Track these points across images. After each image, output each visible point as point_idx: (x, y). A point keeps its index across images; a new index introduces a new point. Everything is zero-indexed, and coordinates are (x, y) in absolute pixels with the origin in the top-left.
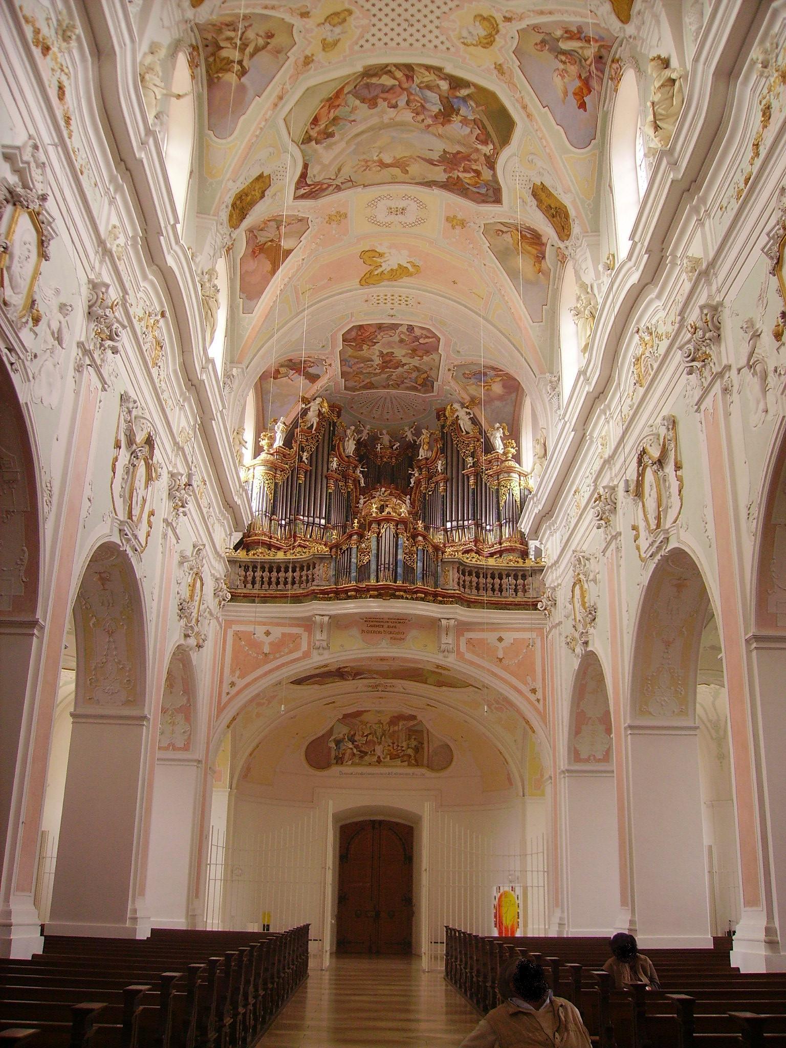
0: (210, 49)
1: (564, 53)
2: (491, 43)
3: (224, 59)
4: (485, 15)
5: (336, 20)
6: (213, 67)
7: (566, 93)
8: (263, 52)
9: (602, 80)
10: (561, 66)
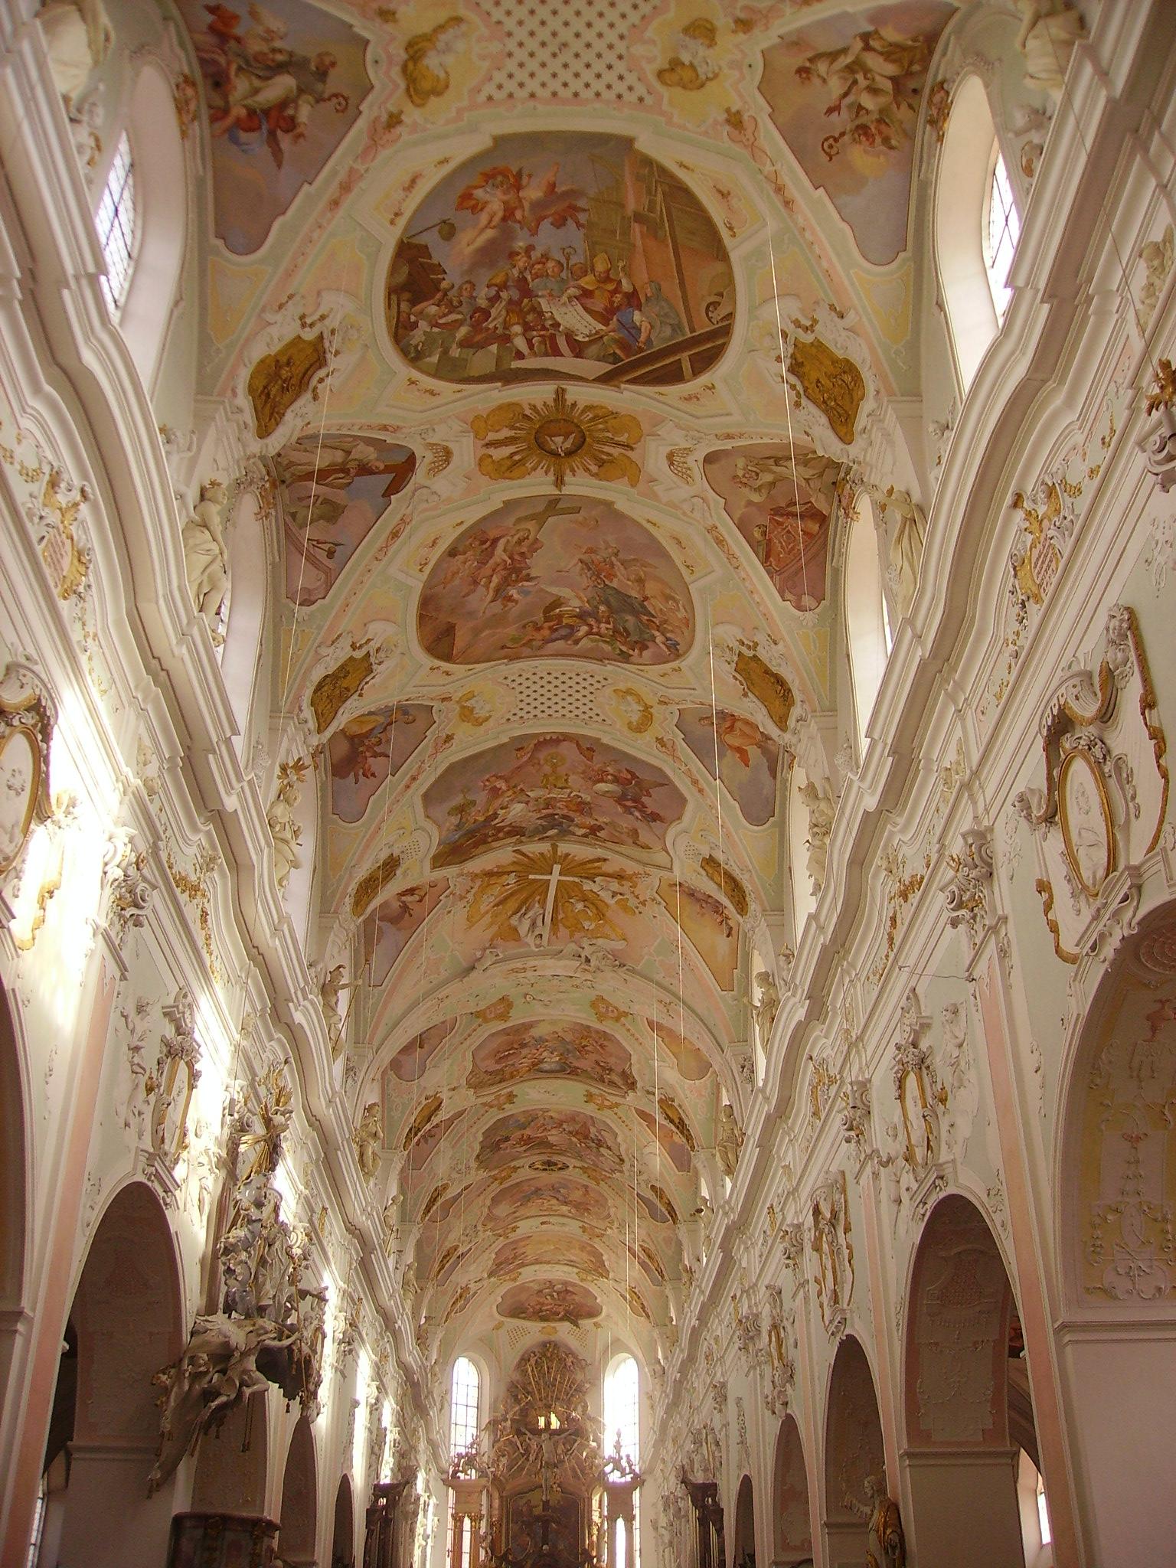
0: (912, 84)
1: (280, 68)
2: (410, 45)
3: (893, 61)
4: (433, 99)
5: (687, 75)
6: (918, 56)
7: (253, 14)
8: (822, 50)
9: (197, 49)
10: (278, 44)
